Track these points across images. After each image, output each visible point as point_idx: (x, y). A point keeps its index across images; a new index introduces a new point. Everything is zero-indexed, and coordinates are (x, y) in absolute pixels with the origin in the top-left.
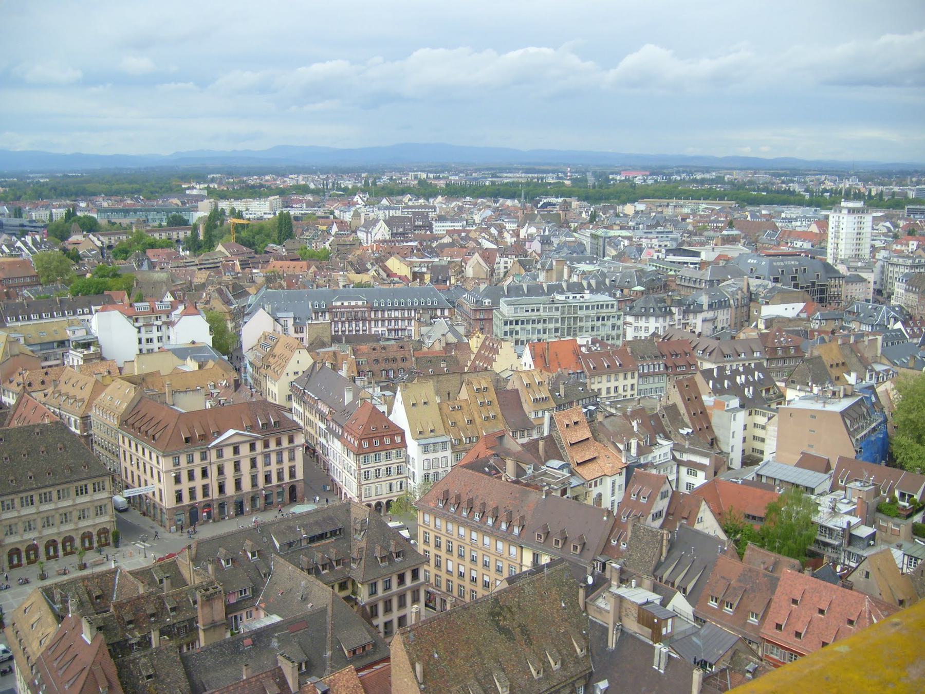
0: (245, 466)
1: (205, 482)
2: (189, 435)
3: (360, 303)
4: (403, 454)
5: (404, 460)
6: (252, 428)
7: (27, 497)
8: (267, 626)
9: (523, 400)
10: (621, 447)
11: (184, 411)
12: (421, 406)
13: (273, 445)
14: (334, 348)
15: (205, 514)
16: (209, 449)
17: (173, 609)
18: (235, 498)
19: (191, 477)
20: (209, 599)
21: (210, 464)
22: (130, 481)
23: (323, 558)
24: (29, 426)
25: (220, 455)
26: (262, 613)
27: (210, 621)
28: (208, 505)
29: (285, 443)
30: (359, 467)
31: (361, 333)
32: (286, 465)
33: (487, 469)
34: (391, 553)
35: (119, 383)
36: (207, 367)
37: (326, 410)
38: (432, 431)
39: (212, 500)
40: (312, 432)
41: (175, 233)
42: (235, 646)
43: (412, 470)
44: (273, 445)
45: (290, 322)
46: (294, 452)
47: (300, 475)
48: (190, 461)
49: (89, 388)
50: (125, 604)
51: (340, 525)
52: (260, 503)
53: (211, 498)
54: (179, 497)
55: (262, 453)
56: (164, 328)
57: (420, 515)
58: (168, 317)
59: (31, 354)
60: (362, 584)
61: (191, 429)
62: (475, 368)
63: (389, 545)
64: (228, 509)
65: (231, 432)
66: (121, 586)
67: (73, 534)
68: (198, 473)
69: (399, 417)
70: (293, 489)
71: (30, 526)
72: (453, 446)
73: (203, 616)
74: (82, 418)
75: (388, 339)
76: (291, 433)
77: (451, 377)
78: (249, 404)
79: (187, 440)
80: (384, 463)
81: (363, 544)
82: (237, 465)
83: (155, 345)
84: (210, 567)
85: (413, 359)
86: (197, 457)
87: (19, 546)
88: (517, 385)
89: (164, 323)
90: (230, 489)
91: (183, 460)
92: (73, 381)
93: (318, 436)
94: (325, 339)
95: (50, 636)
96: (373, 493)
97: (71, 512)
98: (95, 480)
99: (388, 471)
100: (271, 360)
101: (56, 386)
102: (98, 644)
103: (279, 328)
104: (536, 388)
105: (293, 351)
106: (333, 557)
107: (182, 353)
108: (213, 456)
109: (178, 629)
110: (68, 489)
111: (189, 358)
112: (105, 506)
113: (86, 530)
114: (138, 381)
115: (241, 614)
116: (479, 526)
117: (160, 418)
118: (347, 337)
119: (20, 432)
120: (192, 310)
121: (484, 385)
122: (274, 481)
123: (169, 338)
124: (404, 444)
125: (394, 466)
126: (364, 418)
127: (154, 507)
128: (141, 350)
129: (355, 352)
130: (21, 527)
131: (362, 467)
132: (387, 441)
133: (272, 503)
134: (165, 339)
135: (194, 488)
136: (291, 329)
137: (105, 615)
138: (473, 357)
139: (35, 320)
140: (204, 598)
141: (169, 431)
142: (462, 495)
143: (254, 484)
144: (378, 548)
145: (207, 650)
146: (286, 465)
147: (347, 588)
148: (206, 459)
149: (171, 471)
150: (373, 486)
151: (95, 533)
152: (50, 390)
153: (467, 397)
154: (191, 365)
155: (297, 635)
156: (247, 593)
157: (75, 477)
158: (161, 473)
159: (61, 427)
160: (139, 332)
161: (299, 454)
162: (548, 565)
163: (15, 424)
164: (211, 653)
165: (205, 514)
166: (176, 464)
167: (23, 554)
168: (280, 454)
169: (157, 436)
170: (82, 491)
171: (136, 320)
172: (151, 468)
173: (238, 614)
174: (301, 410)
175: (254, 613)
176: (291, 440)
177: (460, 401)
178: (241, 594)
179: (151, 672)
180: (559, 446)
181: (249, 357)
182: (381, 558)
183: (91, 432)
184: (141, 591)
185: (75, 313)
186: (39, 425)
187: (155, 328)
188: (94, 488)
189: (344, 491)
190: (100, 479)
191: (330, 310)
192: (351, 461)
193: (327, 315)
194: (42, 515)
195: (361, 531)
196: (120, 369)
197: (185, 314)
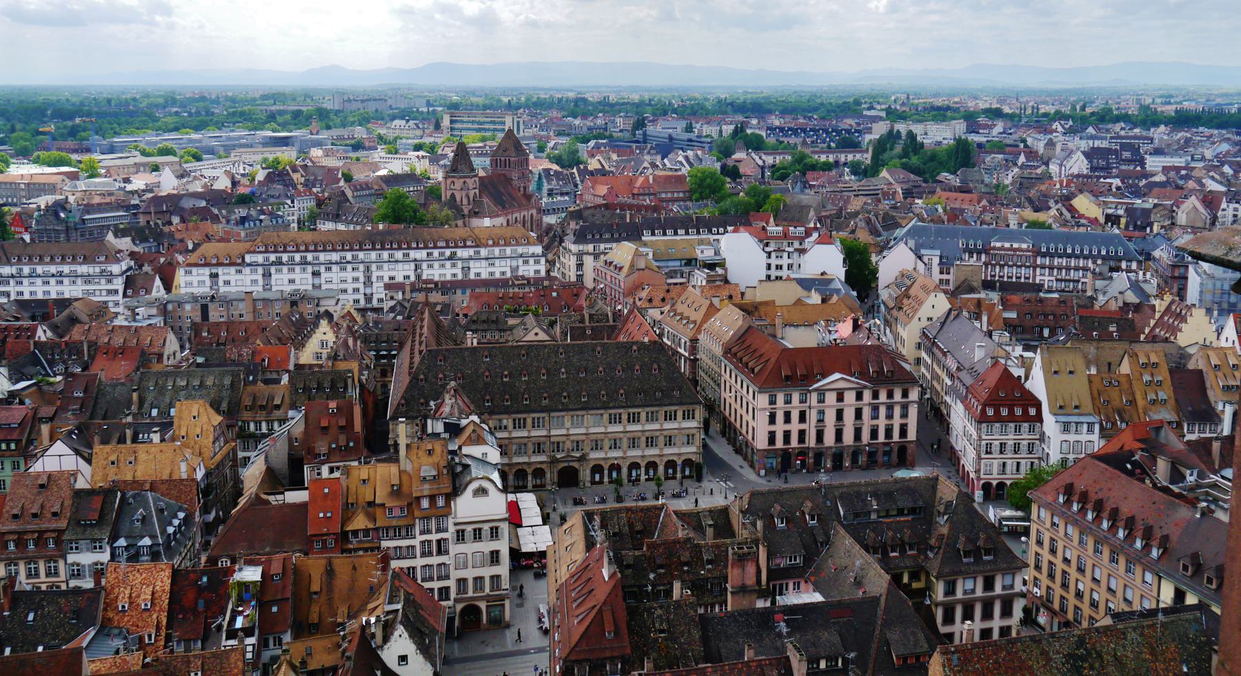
0: (849, 416)
1: (803, 426)
2: (790, 373)
3: (1024, 246)
4: (1037, 429)
5: (1038, 437)
6: (863, 375)
7: (615, 415)
8: (805, 604)
9: (1208, 385)
11: (791, 347)
12: (1064, 376)
13: (883, 397)
14: (982, 295)
15: (798, 462)
16: (810, 392)
17: (709, 562)
18: (833, 450)
19: (787, 419)
20: (741, 559)
21: (810, 408)
22: (727, 414)
23: (893, 539)
24: (627, 343)
25: (821, 401)
26: (811, 587)
27: (740, 583)
28: (803, 453)
29: (898, 396)
30: (980, 437)
31: (1014, 280)
32: (897, 422)
33: (1129, 466)
34: (979, 548)
36: (831, 302)
37: (953, 366)
38: (1076, 407)
39: (808, 448)
40: (939, 389)
41: (843, 156)
42: (766, 619)
43: (1047, 450)
44: (883, 397)
45: (936, 260)
46: (907, 408)
47: (912, 435)
48: (788, 402)
49: (703, 310)
51: (920, 503)
52: (862, 459)
54: (772, 438)
55: (870, 404)
57: (1034, 508)
58: (801, 244)
59: (657, 269)
60: (937, 578)
61: (793, 368)
62: (1155, 337)
63: (978, 538)
64: (825, 461)
65: (837, 376)
66: (664, 525)
67: (657, 460)
68: (795, 416)
69: (1037, 385)
70: (903, 449)
71: (615, 444)
72: (1102, 429)
73: (734, 576)
74: (691, 340)
75: (1050, 291)
76: (906, 386)
77: (1116, 344)
79: (787, 378)
80: (1011, 436)
81: (945, 531)
82: (840, 415)
83: (784, 273)
84: (759, 524)
85: (1077, 318)
86: (796, 397)
87: (602, 463)
88: (1201, 365)
89: (796, 250)
90: (829, 439)
91: (780, 398)
92: (689, 301)
93: (943, 394)
94: (975, 284)
95: (577, 563)
96: (995, 470)
97: (657, 437)
98: (685, 408)
99: (1017, 448)
100: (905, 301)
101: (673, 305)
102: (612, 583)
103: (921, 266)
104: (1228, 371)
105: (928, 293)
106: (906, 539)
107: (806, 284)
108: (814, 397)
109: (712, 585)
110: (657, 412)
112: (693, 435)
113: (671, 458)
114: (749, 310)
115: (787, 584)
116: (1106, 537)
117: (763, 351)
118: (1003, 284)
119: (618, 348)
120: (825, 240)
121: (1154, 359)
122: (881, 438)
124: (1039, 418)
125: (1025, 443)
126: (992, 380)
127: (747, 446)
128: (768, 277)
129: (1003, 301)
130: (607, 444)
131: (984, 437)
132: (1018, 412)
133: (876, 462)
134: (795, 267)
135: (790, 431)
136: (936, 269)
137: (637, 553)
138: (1152, 322)
139: (670, 237)
140: (736, 557)
141: (770, 366)
142: (1089, 493)
144: (962, 539)
145: (731, 616)
146: (897, 422)
147: (919, 580)
148: (806, 402)
149: (765, 409)
150: (995, 462)
151: (679, 462)
152: (667, 309)
153: (1128, 371)
154: (815, 298)
155: (838, 622)
156: (798, 561)
157: (666, 401)
159: (657, 347)
161: (913, 411)
162: (1192, 607)
163: (622, 338)
164: (736, 620)
165: (798, 462)
166: (773, 402)
167: (606, 472)
168: (890, 408)
169: (756, 370)
170: (670, 417)
171: (767, 245)
173: (784, 582)
174: (929, 361)
175: (802, 585)
176: (905, 395)
177: (1120, 375)
178: (790, 561)
179: (665, 626)
181: (884, 294)
182: (965, 552)
183: (698, 357)
184: (680, 536)
185: (710, 231)
187: (785, 255)
188: (684, 415)
189: (962, 462)
190: (691, 407)
191: (986, 250)
192: (972, 430)
193: (983, 257)
194: (628, 435)
195: (945, 514)
196: (743, 294)
197: (820, 242)
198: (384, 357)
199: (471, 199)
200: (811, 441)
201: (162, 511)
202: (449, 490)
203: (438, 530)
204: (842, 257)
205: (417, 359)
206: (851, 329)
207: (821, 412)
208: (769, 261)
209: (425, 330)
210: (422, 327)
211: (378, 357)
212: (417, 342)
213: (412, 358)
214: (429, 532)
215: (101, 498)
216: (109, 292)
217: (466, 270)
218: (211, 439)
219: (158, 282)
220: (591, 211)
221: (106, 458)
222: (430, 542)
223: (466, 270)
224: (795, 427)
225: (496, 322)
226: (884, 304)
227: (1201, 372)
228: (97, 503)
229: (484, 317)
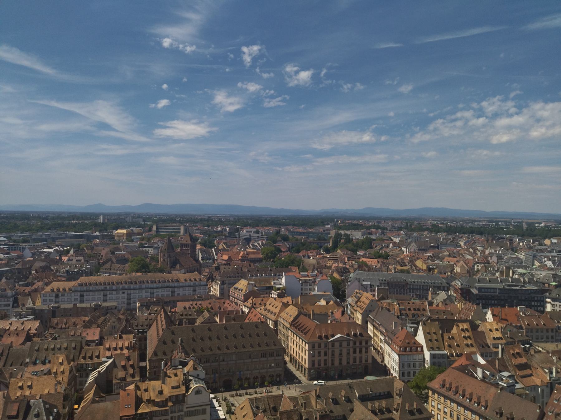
0: (345, 352)
1: (326, 358)
10: (547, 371)
13: (358, 344)
15: (324, 374)
25: (333, 346)
33: (466, 371)
35: (291, 306)
40: (377, 340)
49: (279, 308)
50: (284, 413)
53: (327, 366)
55: (352, 347)
56: (312, 284)
68: (322, 353)
74: (274, 321)
78: (348, 323)
83: (308, 292)
88: (483, 329)
89: (313, 282)
90: (337, 363)
92: (272, 304)
93: (379, 343)
101: (265, 306)
111: (322, 299)
117: (308, 325)
122: (358, 362)
123: (314, 289)
128: (302, 294)
134: (312, 289)
137: (275, 417)
143: (348, 363)
144: (407, 405)
152: (263, 308)
158: (306, 351)
160: (302, 285)
163: (247, 321)
172: (302, 348)
174: (372, 329)
177: (453, 334)
180: (508, 365)
186: (257, 322)
187: (308, 284)
198: (141, 332)
199: (172, 261)
200: (329, 364)
201: (48, 408)
202: (184, 392)
203: (179, 411)
204: (332, 285)
205: (161, 332)
206: (341, 316)
207: (333, 352)
208: (302, 287)
209: (163, 319)
210: (161, 318)
211: (139, 332)
212: (160, 325)
213: (158, 332)
214: (175, 412)
215: (18, 404)
216: (6, 305)
217: (173, 292)
218: (68, 373)
219: (30, 300)
220: (224, 266)
221: (17, 385)
222: (175, 417)
223: (173, 292)
224: (323, 358)
225: (190, 315)
226: (350, 305)
227: (484, 331)
228: (16, 407)
229: (186, 313)
